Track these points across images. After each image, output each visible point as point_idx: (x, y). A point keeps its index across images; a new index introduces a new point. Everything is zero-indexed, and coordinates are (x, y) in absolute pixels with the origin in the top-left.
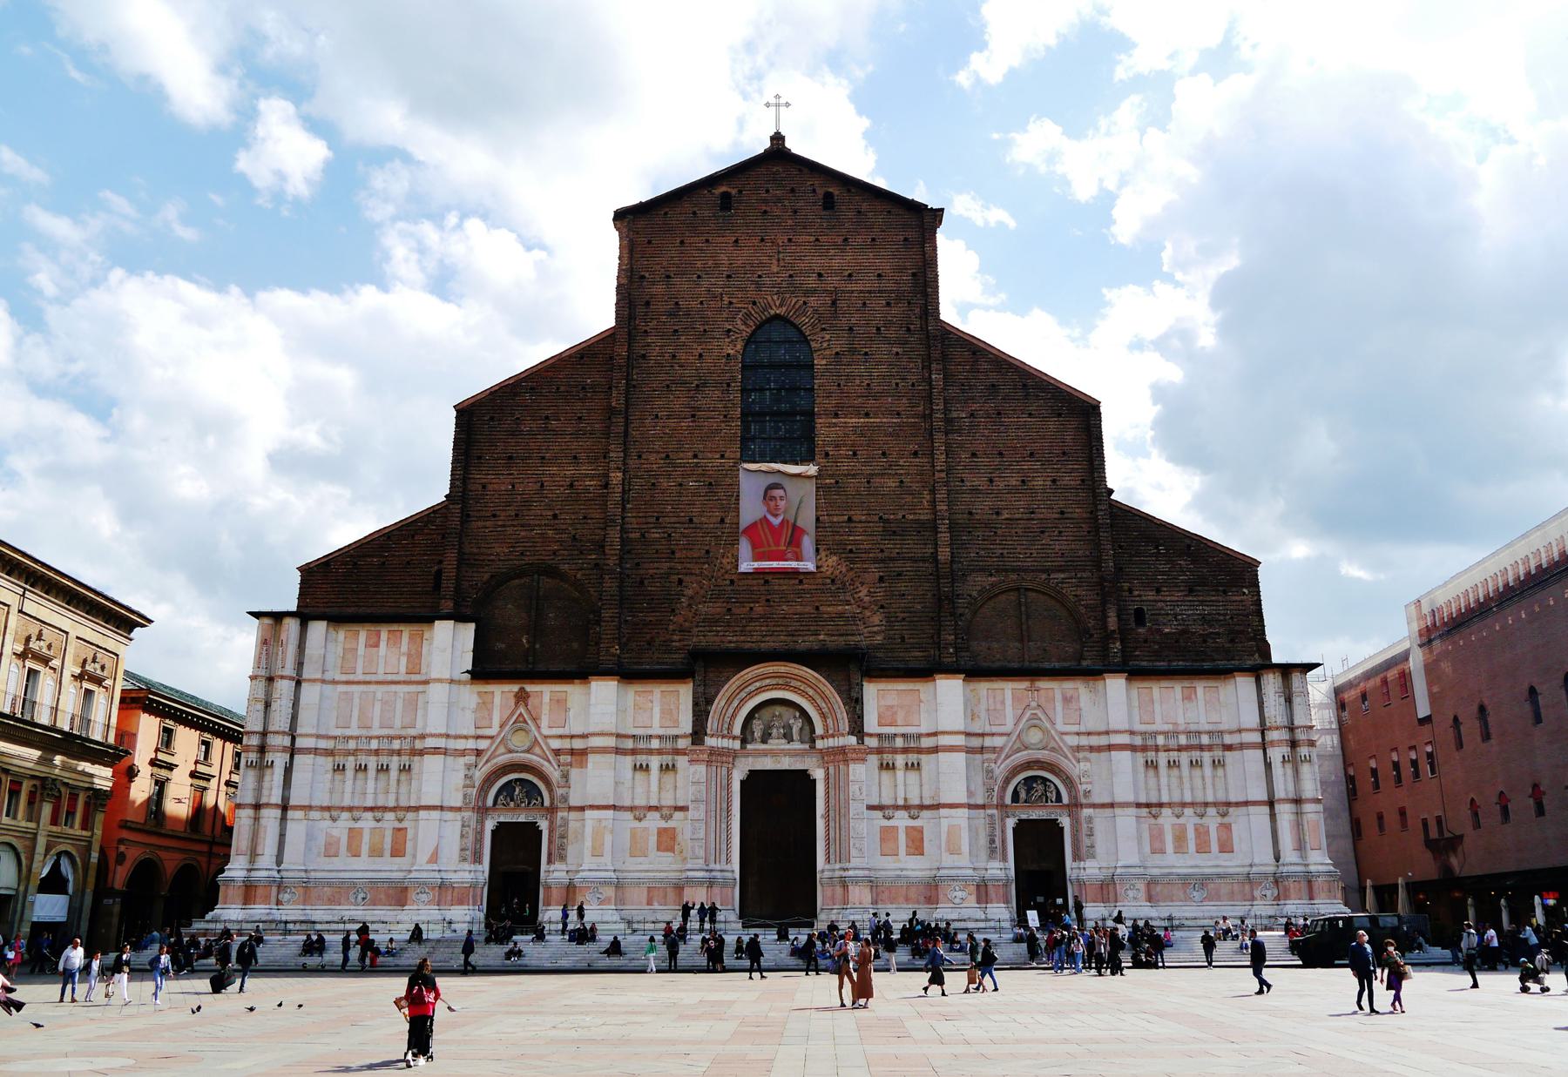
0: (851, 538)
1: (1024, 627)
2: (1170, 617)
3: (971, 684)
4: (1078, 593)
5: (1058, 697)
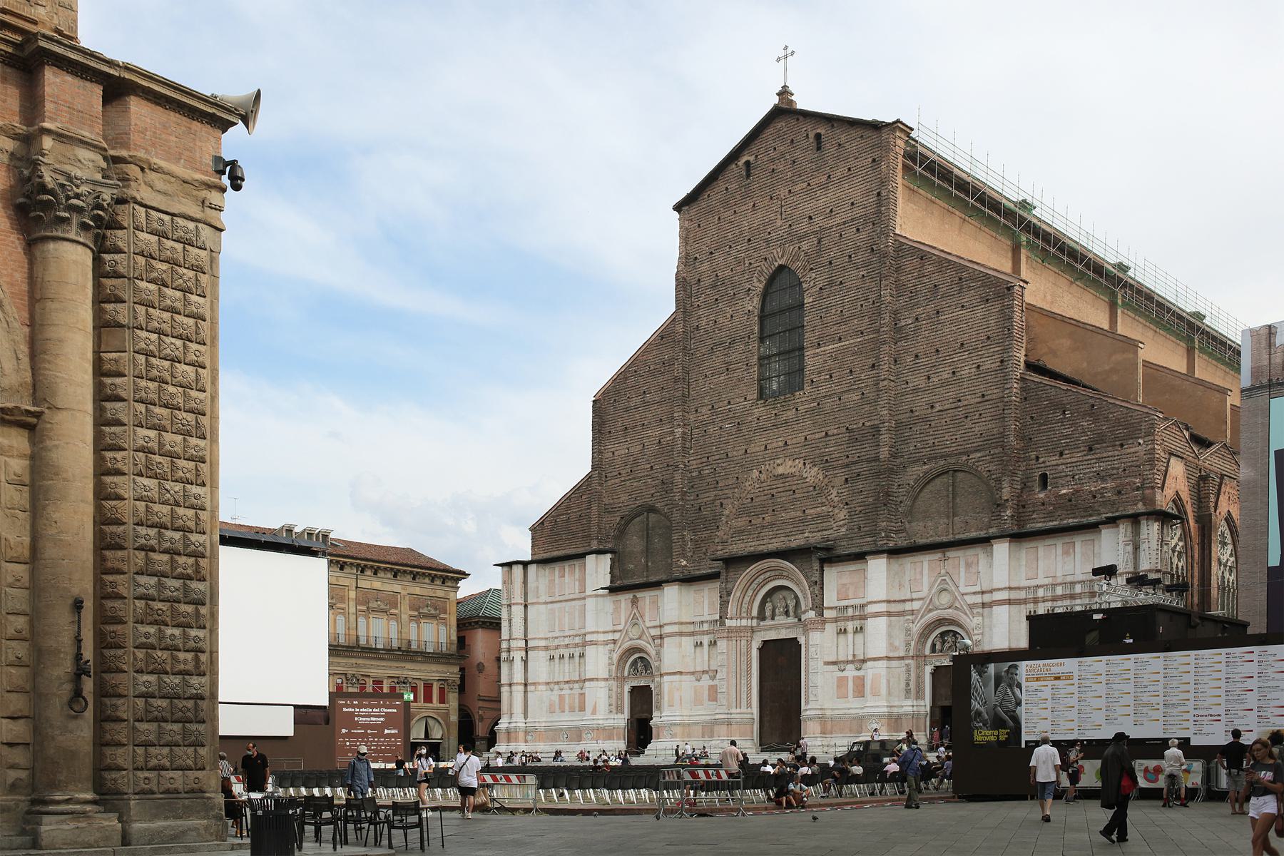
0: (827, 450)
1: (951, 505)
2: (1068, 478)
3: (900, 560)
4: (990, 468)
5: (962, 563)
